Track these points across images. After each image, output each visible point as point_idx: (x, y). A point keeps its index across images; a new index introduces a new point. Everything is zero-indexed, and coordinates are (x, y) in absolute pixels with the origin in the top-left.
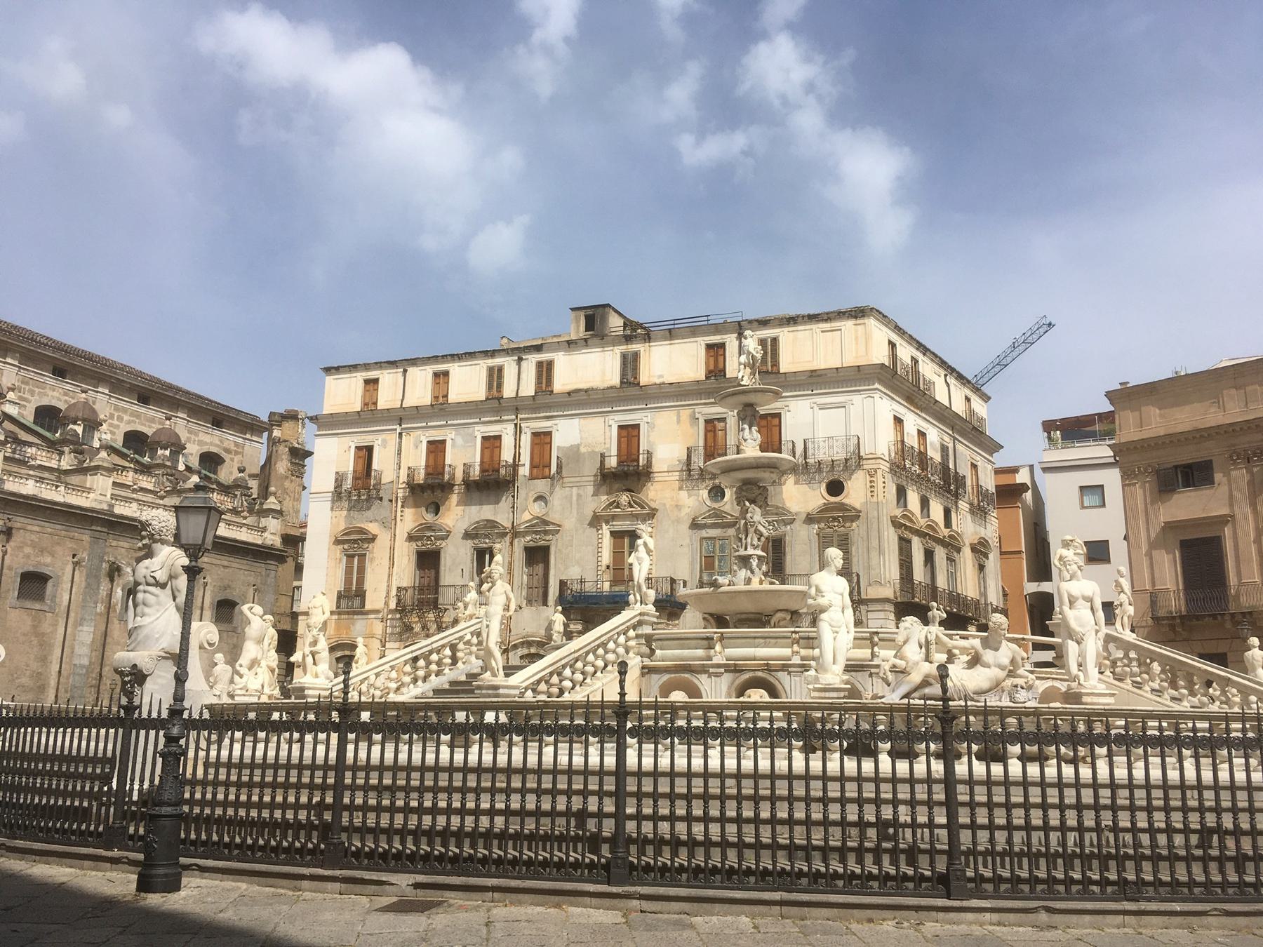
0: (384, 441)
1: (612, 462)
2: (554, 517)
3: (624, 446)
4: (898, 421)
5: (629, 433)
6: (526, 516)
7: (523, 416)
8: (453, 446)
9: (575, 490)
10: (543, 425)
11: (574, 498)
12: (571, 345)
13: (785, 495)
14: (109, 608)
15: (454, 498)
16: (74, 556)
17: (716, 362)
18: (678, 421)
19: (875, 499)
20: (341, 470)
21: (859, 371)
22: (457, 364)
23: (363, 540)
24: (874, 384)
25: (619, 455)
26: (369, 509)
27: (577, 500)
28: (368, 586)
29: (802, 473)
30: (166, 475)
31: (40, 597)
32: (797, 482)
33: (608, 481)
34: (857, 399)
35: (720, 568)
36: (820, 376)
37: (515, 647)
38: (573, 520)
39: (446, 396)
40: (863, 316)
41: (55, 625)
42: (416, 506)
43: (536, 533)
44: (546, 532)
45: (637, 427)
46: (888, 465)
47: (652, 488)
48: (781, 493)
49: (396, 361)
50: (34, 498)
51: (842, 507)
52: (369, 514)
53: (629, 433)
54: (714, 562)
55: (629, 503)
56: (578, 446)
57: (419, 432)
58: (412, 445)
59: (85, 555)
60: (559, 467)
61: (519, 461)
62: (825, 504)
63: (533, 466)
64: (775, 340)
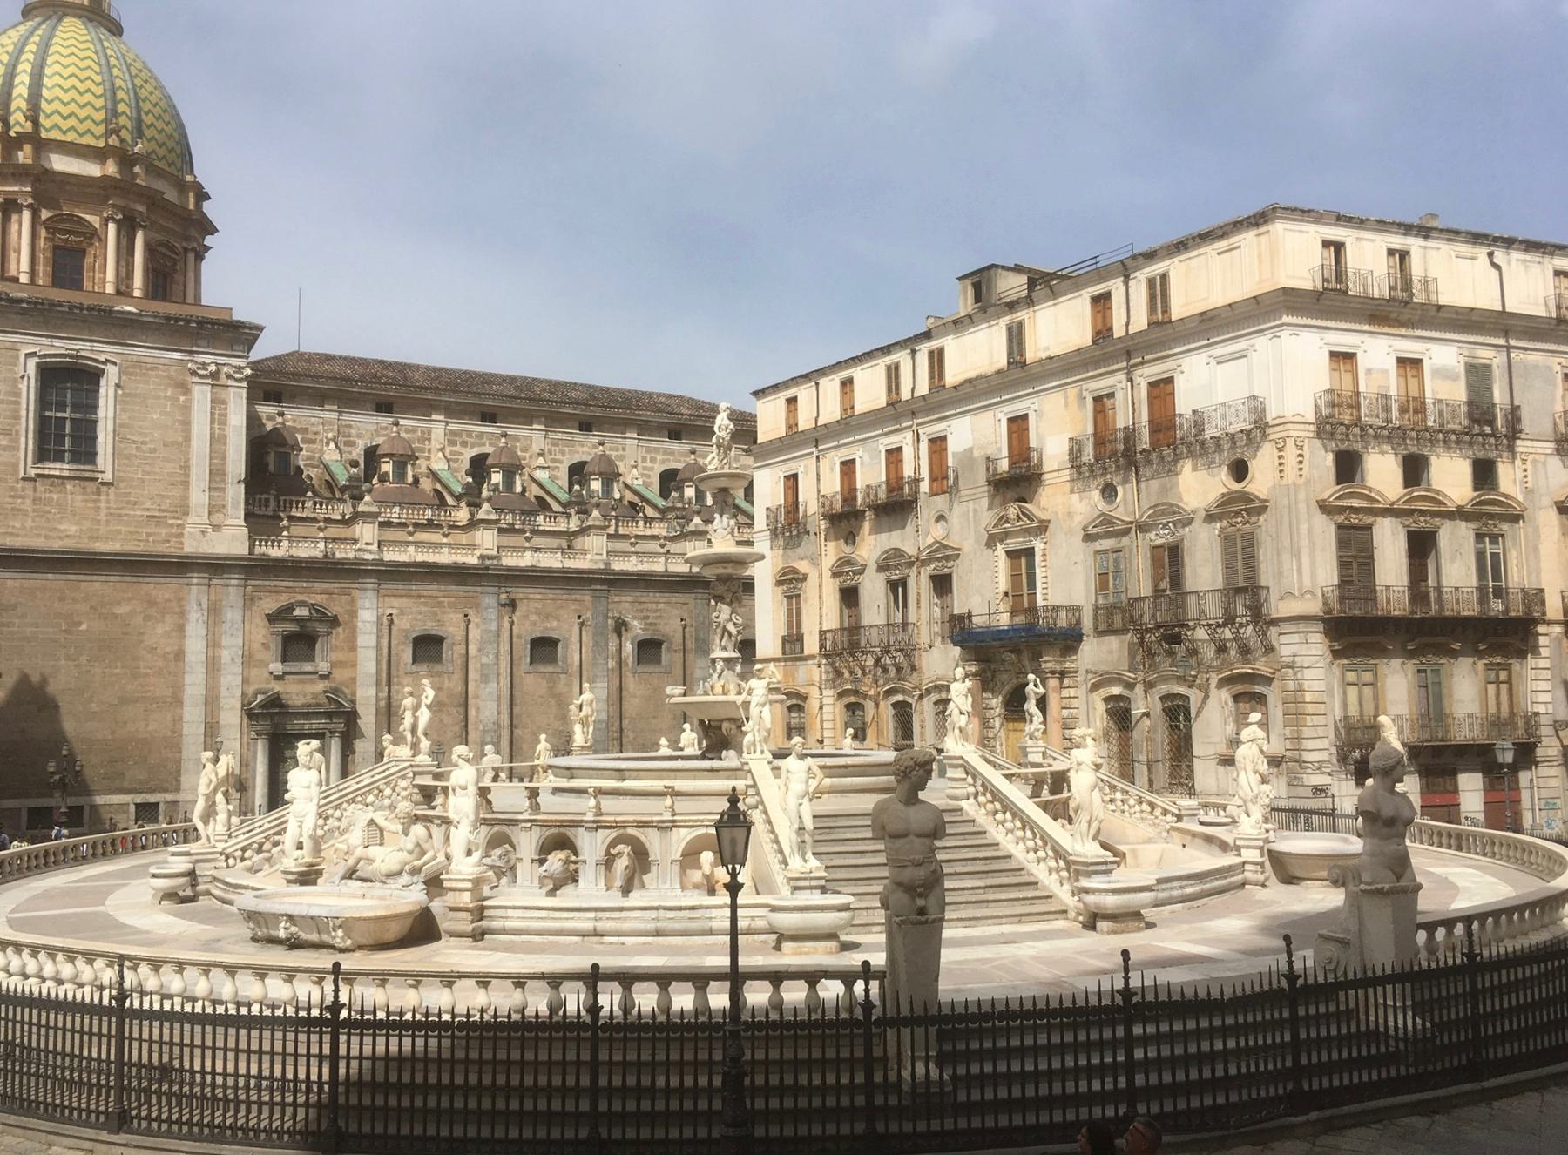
0: (806, 467)
1: (1004, 465)
3: (1015, 443)
4: (1343, 358)
5: (1018, 424)
7: (920, 421)
8: (862, 464)
10: (936, 429)
11: (971, 514)
12: (958, 325)
13: (1182, 488)
14: (620, 663)
15: (867, 526)
16: (579, 617)
17: (1104, 318)
18: (1066, 405)
19: (1284, 482)
20: (773, 504)
21: (1258, 303)
23: (797, 579)
24: (1281, 318)
25: (1010, 456)
26: (800, 545)
28: (805, 630)
29: (1201, 455)
30: (677, 518)
31: (552, 659)
32: (1194, 469)
34: (1261, 342)
35: (1115, 588)
36: (1212, 318)
37: (928, 691)
39: (852, 408)
40: (1266, 222)
41: (570, 685)
42: (837, 539)
43: (939, 559)
44: (947, 558)
45: (1025, 417)
46: (1312, 428)
48: (1177, 484)
50: (533, 569)
51: (1244, 497)
52: (800, 551)
53: (1018, 424)
54: (1108, 581)
56: (971, 450)
57: (832, 453)
59: (589, 615)
60: (956, 478)
62: (1224, 495)
63: (933, 479)
64: (1164, 277)
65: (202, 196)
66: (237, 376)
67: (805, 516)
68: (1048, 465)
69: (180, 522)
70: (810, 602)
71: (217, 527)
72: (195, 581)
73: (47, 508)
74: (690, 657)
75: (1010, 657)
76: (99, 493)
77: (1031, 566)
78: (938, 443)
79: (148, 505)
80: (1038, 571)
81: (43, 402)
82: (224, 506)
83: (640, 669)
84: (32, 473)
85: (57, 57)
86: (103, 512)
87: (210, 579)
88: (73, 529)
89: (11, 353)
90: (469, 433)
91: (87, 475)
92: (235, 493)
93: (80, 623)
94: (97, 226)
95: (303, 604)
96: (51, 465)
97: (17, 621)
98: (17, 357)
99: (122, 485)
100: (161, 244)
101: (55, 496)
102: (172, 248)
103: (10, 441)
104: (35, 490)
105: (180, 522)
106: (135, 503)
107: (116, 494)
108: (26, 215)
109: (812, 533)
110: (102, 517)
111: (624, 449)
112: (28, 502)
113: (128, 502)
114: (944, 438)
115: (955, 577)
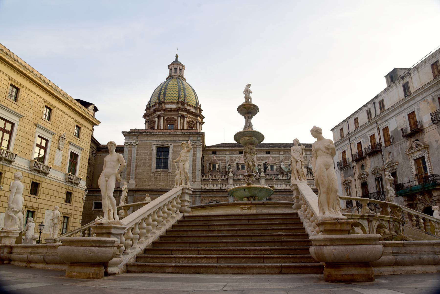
0: (347, 148)
1: (409, 131)
2: (396, 159)
5: (412, 115)
6: (387, 161)
8: (363, 143)
9: (399, 146)
10: (385, 125)
11: (400, 150)
20: (338, 161)
22: (359, 114)
23: (349, 183)
27: (401, 150)
33: (409, 139)
38: (401, 158)
47: (425, 137)
49: (344, 120)
53: (412, 115)
55: (416, 146)
56: (397, 129)
58: (354, 147)
60: (393, 139)
61: (381, 141)
63: (385, 141)
65: (201, 110)
66: (198, 145)
67: (349, 163)
68: (426, 126)
70: (353, 190)
71: (194, 182)
73: (157, 179)
75: (420, 197)
76: (168, 175)
77: (424, 163)
78: (386, 130)
80: (427, 164)
81: (157, 155)
82: (196, 177)
84: (154, 171)
85: (170, 85)
89: (151, 145)
90: (263, 157)
91: (166, 171)
92: (199, 173)
94: (176, 119)
95: (214, 201)
96: (158, 169)
98: (152, 146)
99: (173, 173)
100: (190, 121)
101: (159, 176)
102: (193, 122)
103: (150, 164)
104: (155, 175)
107: (172, 175)
108: (162, 118)
109: (351, 168)
110: (169, 181)
111: (306, 158)
112: (153, 178)
114: (387, 127)
115: (397, 172)
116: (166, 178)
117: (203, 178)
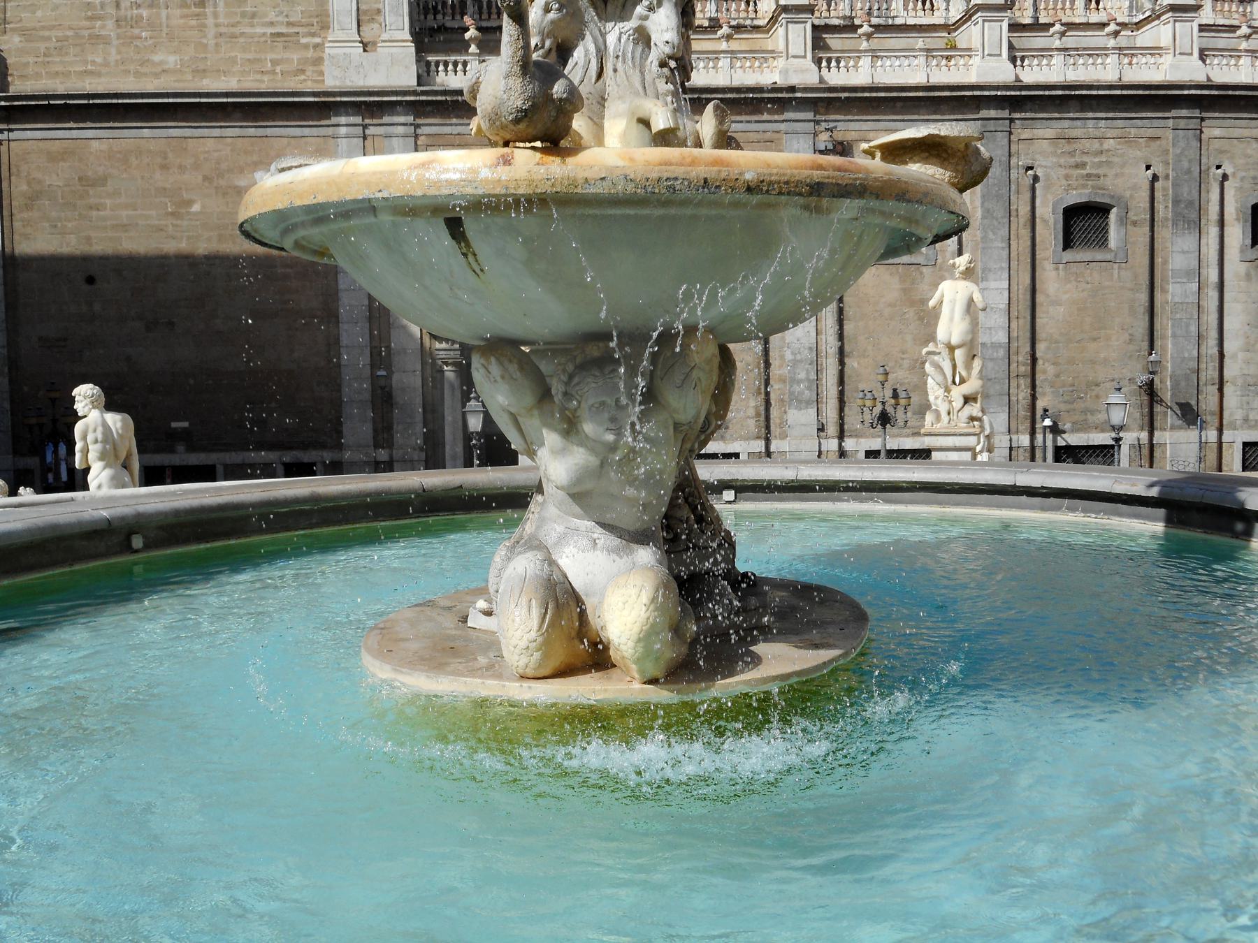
69: (317, 40)
72: (343, 130)
73: (136, 31)
74: (1163, 233)
79: (272, 16)
82: (379, 11)
83: (1069, 255)
86: (211, 32)
87: (365, 127)
88: (172, 60)
93: (190, 203)
97: (108, 202)
101: (145, 13)
105: (317, 40)
106: (254, 15)
112: (110, 24)
113: (243, 15)
116: (194, 23)
117: (431, 17)
